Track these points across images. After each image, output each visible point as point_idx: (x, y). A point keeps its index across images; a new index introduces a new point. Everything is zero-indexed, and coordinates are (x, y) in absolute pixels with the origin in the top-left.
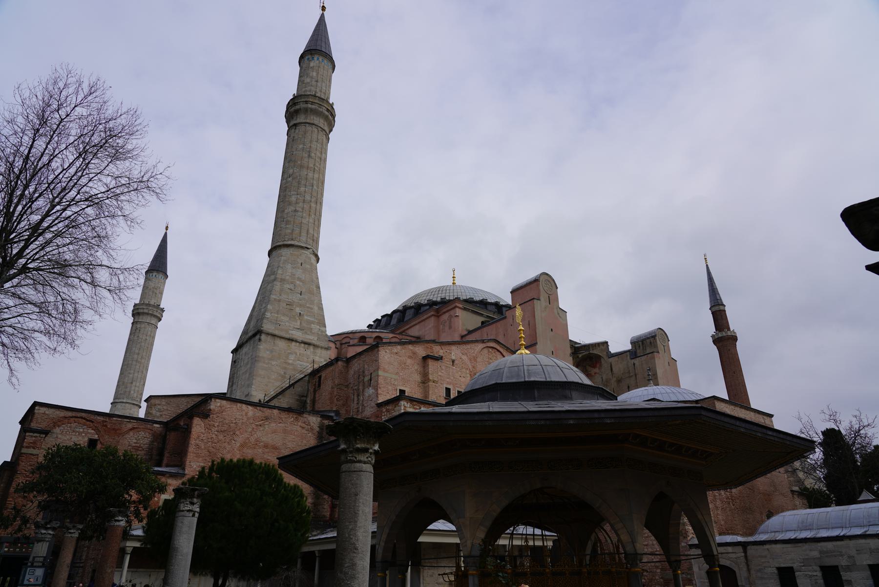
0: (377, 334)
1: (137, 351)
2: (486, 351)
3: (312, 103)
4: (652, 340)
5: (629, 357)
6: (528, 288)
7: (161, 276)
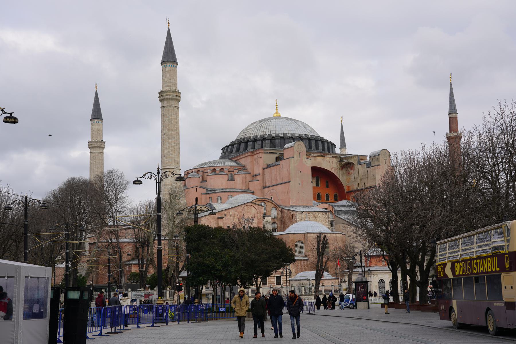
0: (221, 167)
1: (96, 170)
2: (246, 207)
3: (169, 95)
4: (378, 156)
6: (289, 149)
7: (100, 121)
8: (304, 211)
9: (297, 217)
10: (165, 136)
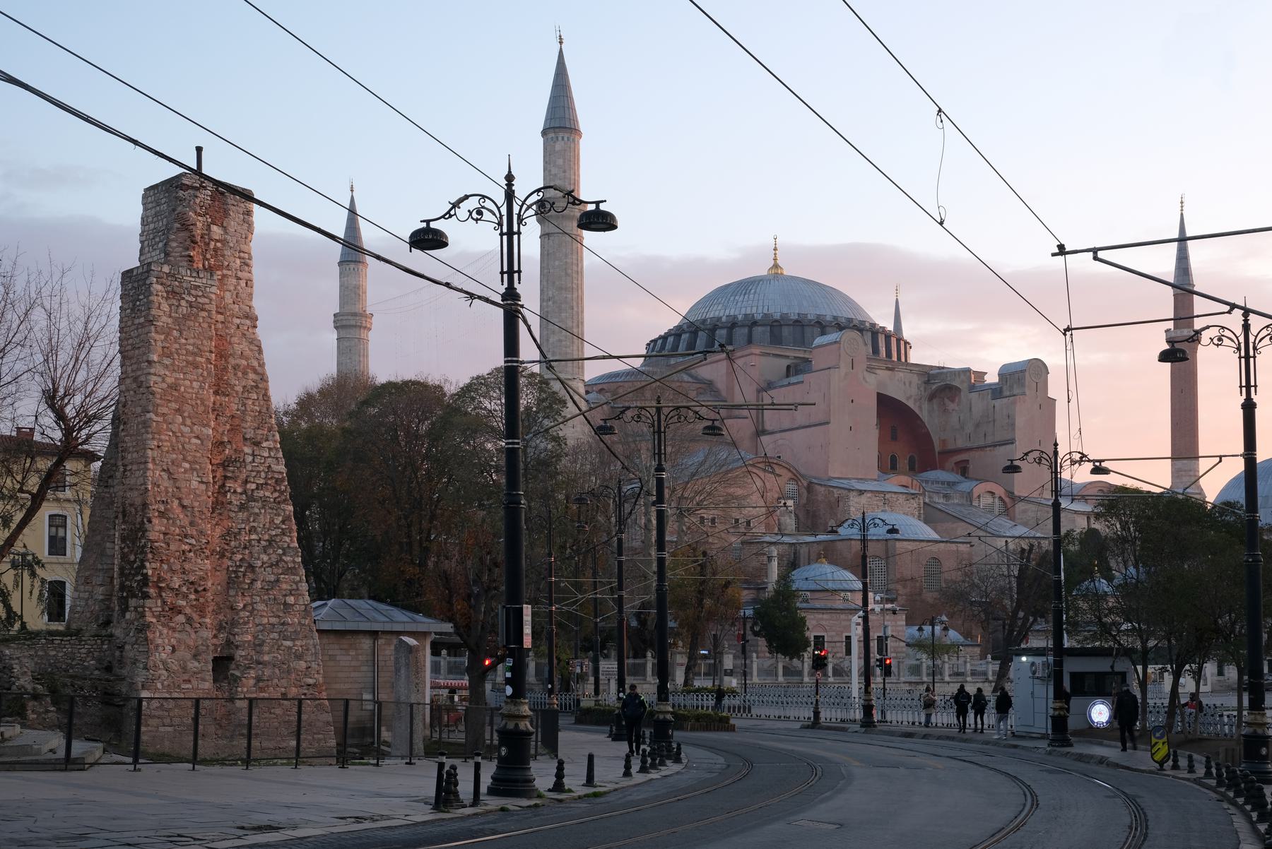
5: (989, 397)
8: (865, 491)
9: (851, 503)
10: (550, 303)
